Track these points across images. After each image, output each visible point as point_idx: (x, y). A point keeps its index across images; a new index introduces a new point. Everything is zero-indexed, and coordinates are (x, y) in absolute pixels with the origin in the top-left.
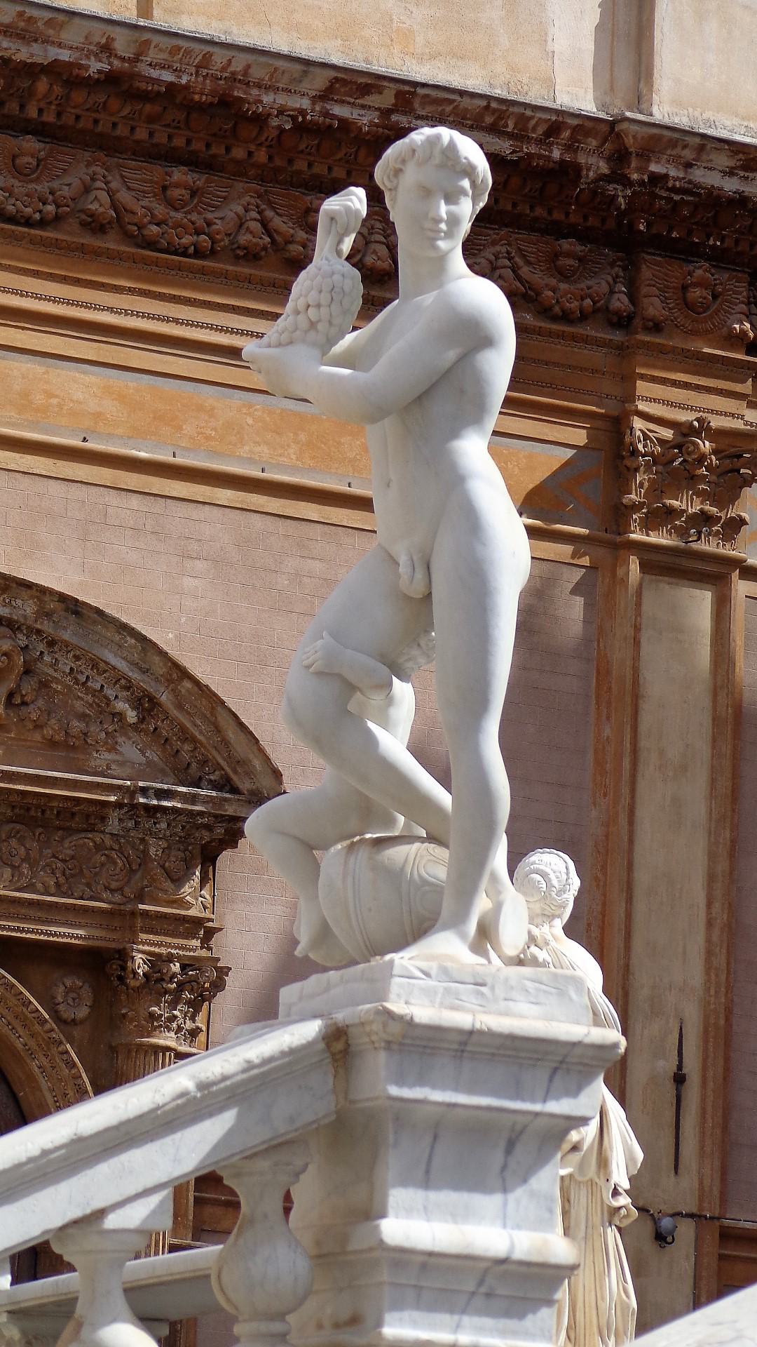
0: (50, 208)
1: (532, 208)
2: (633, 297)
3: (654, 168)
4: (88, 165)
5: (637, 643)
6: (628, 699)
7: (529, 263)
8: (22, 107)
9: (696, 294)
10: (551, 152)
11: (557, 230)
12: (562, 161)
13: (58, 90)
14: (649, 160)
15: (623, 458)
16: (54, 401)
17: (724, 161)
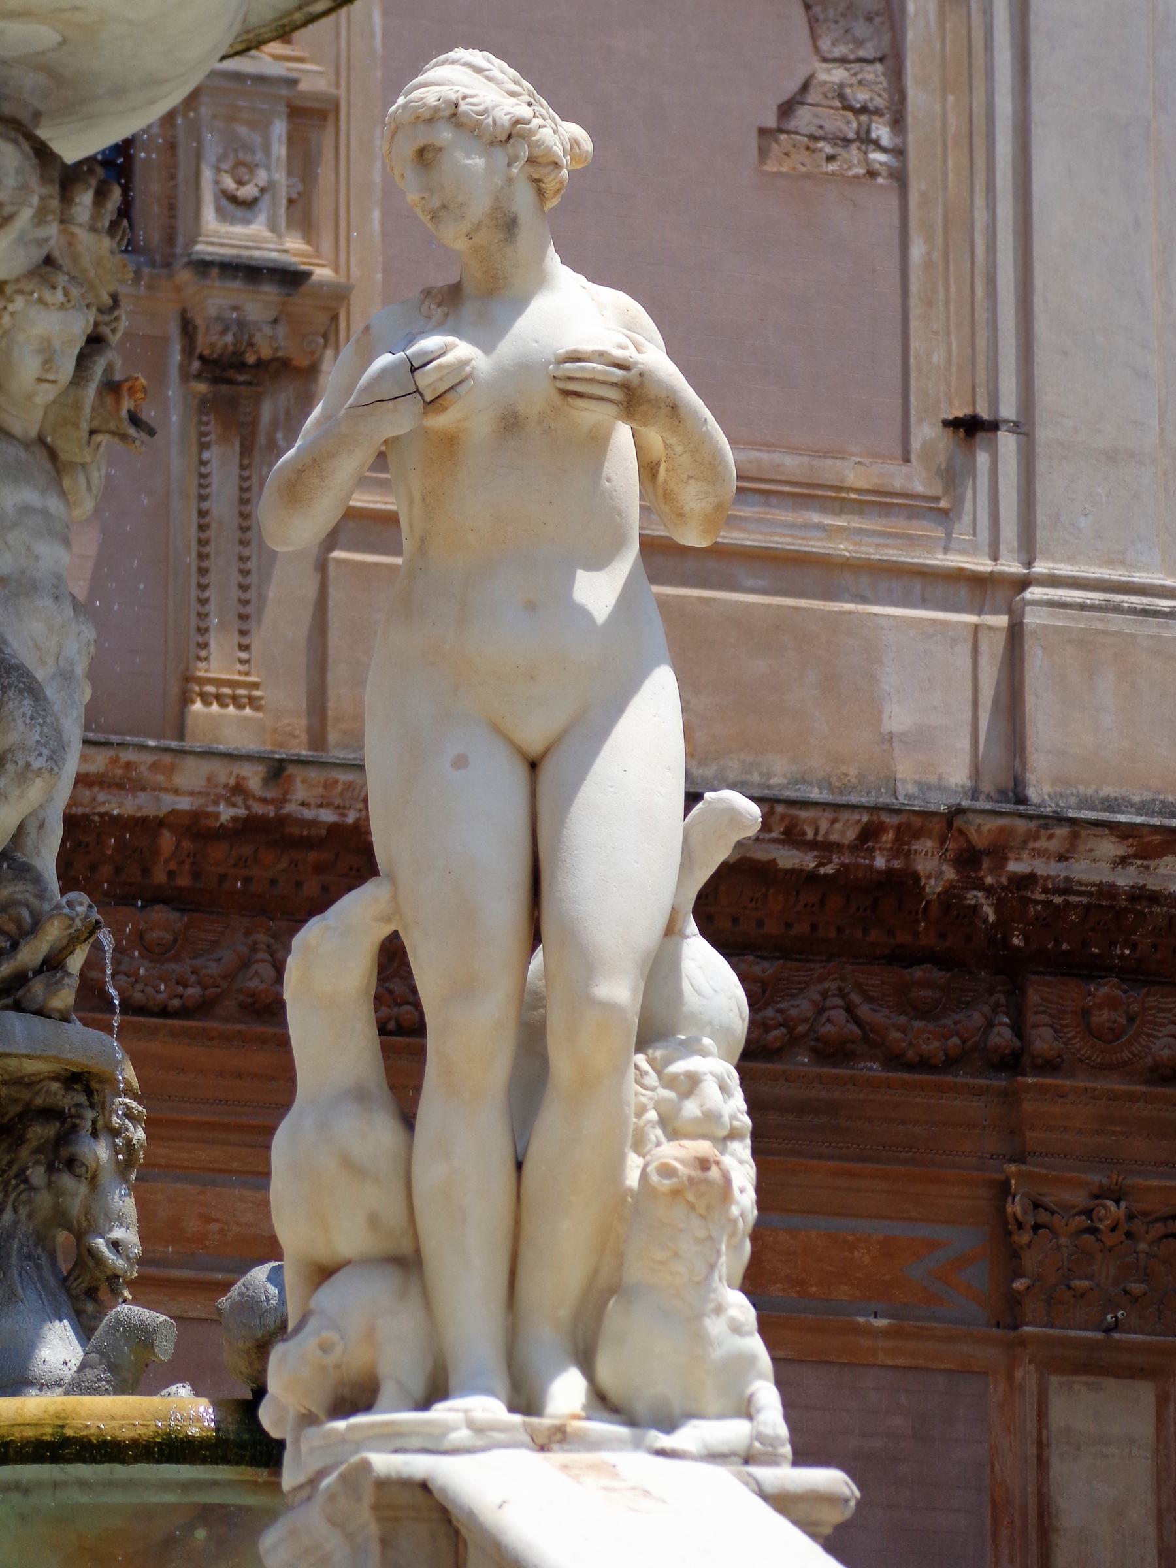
0: (193, 992)
1: (865, 931)
2: (1019, 1029)
3: (1013, 867)
4: (248, 933)
5: (1042, 1464)
6: (1033, 1535)
7: (870, 999)
8: (146, 872)
9: (1103, 1017)
10: (873, 859)
11: (903, 957)
12: (890, 872)
13: (187, 845)
14: (1005, 859)
15: (1010, 1233)
16: (214, 1227)
17: (1109, 848)
